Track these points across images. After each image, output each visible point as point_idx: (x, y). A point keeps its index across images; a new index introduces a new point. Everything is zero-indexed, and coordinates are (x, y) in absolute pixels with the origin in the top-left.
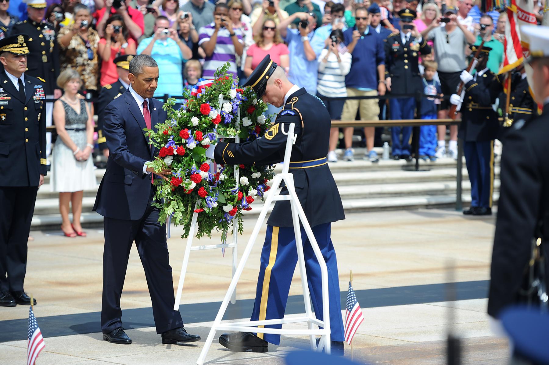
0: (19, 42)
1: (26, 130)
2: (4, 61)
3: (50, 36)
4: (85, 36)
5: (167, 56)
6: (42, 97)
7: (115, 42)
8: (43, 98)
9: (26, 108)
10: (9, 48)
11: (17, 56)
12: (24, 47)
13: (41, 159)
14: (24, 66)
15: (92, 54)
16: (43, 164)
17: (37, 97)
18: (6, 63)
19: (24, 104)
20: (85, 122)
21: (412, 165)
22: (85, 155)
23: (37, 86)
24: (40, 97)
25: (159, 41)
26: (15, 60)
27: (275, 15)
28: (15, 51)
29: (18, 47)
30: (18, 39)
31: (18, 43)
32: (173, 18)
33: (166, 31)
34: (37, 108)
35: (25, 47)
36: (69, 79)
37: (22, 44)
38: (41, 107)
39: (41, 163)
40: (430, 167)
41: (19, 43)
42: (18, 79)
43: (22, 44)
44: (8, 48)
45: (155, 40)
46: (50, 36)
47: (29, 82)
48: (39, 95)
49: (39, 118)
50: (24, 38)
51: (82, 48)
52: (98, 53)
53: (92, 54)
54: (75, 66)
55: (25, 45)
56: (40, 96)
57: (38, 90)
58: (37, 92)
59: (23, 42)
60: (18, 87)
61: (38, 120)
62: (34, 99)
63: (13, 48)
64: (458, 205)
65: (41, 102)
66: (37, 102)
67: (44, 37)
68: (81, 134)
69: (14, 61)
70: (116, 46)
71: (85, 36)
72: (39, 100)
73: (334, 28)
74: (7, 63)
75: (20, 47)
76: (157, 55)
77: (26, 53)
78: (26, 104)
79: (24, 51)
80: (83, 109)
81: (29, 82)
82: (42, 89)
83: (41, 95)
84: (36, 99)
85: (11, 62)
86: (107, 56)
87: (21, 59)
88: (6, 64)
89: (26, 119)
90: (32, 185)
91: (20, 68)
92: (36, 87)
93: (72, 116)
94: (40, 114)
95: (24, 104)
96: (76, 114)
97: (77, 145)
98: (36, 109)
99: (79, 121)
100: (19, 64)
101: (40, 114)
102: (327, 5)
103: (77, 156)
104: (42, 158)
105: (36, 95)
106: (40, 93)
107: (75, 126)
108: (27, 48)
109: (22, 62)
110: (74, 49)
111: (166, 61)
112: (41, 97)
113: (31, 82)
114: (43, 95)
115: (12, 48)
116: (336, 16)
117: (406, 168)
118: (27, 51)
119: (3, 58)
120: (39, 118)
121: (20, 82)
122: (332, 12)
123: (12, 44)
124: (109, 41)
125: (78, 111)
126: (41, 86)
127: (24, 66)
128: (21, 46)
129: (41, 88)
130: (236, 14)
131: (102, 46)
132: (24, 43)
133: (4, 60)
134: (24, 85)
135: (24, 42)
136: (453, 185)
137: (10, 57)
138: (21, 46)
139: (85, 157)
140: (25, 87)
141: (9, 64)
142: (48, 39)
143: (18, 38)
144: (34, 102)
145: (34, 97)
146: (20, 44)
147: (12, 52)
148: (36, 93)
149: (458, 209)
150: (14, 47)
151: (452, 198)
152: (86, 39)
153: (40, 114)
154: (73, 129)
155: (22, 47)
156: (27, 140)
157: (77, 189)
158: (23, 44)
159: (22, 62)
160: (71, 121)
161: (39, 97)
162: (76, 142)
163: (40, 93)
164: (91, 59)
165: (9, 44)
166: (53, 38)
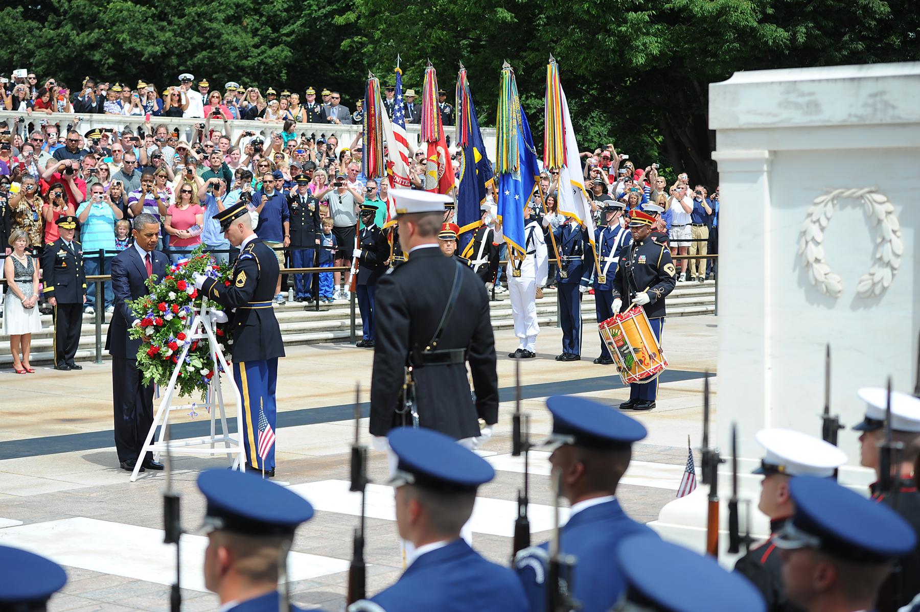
4: (30, 201)
5: (102, 217)
7: (57, 206)
15: (37, 216)
21: (313, 306)
25: (95, 205)
27: (193, 181)
32: (105, 184)
33: (101, 196)
40: (329, 307)
45: (92, 203)
52: (42, 215)
53: (37, 216)
54: (22, 226)
64: (351, 339)
70: (58, 209)
71: (30, 201)
73: (244, 191)
76: (93, 216)
86: (50, 218)
102: (237, 172)
111: (101, 222)
116: (245, 182)
117: (307, 309)
122: (242, 178)
124: (51, 205)
130: (161, 181)
131: (46, 209)
136: (348, 322)
149: (352, 343)
151: (348, 333)
152: (32, 204)
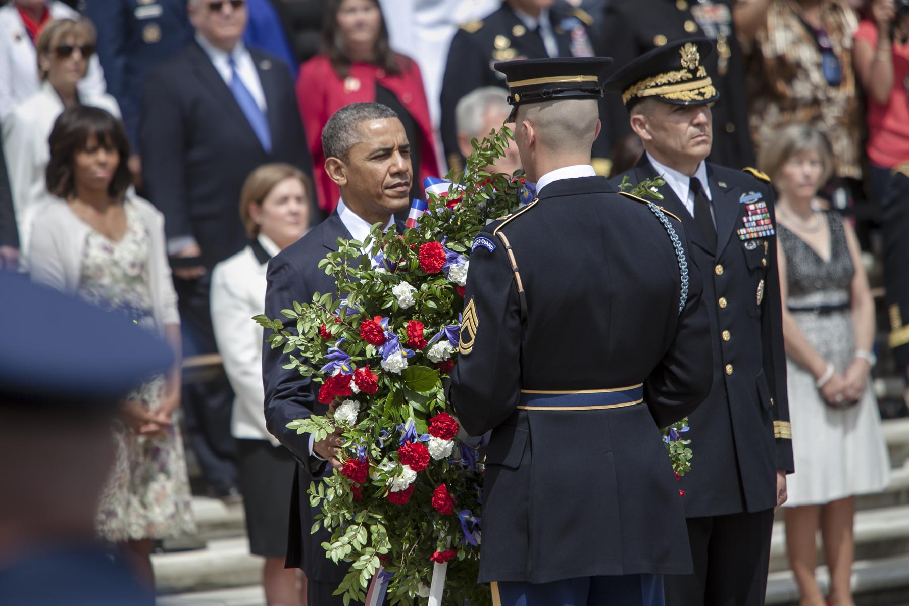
0: (684, 64)
1: (726, 335)
2: (645, 128)
3: (716, 26)
6: (766, 227)
8: (768, 233)
9: (719, 269)
10: (657, 86)
11: (680, 108)
12: (701, 78)
13: (775, 423)
14: (704, 138)
15: (839, 69)
16: (780, 439)
17: (751, 230)
18: (650, 134)
19: (714, 256)
20: (846, 282)
22: (852, 386)
23: (748, 194)
24: (758, 229)
26: (678, 122)
28: (674, 93)
29: (682, 81)
30: (681, 56)
31: (679, 68)
34: (752, 267)
35: (704, 78)
36: (788, 153)
37: (694, 71)
38: (764, 260)
39: (777, 436)
41: (685, 68)
42: (688, 180)
43: (694, 71)
44: (653, 87)
46: (716, 26)
47: (723, 185)
48: (754, 224)
49: (760, 295)
50: (698, 50)
51: (807, 54)
53: (839, 69)
54: (789, 105)
55: (702, 72)
56: (758, 224)
57: (752, 207)
58: (750, 213)
59: (697, 62)
60: (690, 205)
61: (759, 302)
62: (743, 238)
63: (669, 84)
65: (763, 246)
66: (753, 246)
67: (700, 31)
68: (835, 323)
69: (672, 125)
72: (758, 238)
74: (654, 133)
75: (689, 80)
77: (708, 96)
78: (718, 255)
79: (702, 91)
80: (838, 243)
81: (723, 185)
82: (763, 204)
83: (762, 222)
84: (748, 236)
85: (665, 129)
87: (695, 118)
88: (650, 137)
89: (723, 302)
90: (754, 507)
91: (694, 146)
92: (744, 199)
93: (805, 268)
94: (762, 282)
95: (714, 256)
96: (818, 259)
97: (828, 356)
98: (749, 269)
99: (828, 282)
100: (688, 134)
101: (761, 284)
103: (829, 390)
104: (778, 419)
105: (747, 225)
106: (758, 217)
107: (816, 299)
108: (708, 81)
109: (698, 125)
110: (781, 59)
112: (762, 228)
113: (727, 184)
114: (767, 221)
115: (664, 84)
118: (710, 91)
119: (639, 120)
120: (760, 295)
121: (695, 187)
123: (666, 71)
125: (824, 250)
126: (759, 195)
127: (704, 138)
128: (690, 76)
129: (760, 200)
132: (700, 67)
133: (642, 125)
134: (710, 198)
135: (700, 64)
137: (660, 114)
138: (690, 76)
139: (851, 393)
140: (712, 202)
141: (662, 135)
142: (710, 32)
143: (682, 52)
144: (744, 249)
145: (743, 231)
146: (689, 71)
147: (667, 96)
148: (745, 219)
150: (672, 81)
153: (761, 284)
154: (808, 310)
155: (695, 79)
156: (729, 369)
157: (836, 493)
158: (697, 69)
159: (698, 125)
160: (805, 283)
161: (755, 229)
162: (823, 350)
163: (758, 217)
164: (835, 83)
165: (654, 75)
166: (725, 31)
